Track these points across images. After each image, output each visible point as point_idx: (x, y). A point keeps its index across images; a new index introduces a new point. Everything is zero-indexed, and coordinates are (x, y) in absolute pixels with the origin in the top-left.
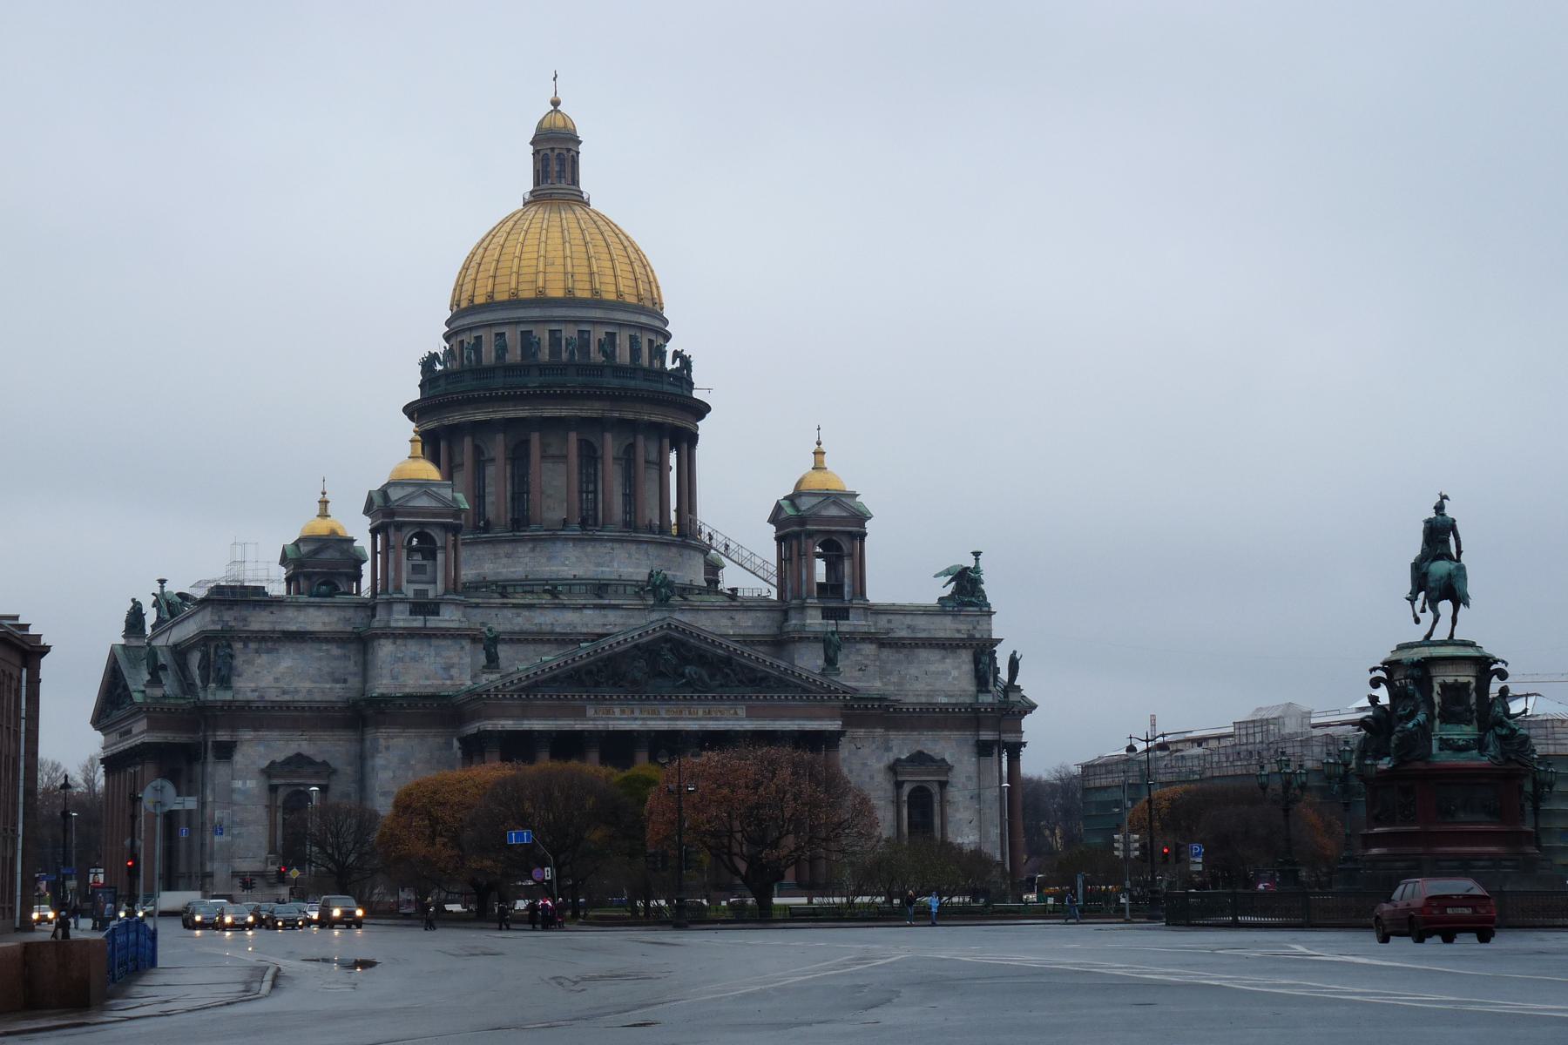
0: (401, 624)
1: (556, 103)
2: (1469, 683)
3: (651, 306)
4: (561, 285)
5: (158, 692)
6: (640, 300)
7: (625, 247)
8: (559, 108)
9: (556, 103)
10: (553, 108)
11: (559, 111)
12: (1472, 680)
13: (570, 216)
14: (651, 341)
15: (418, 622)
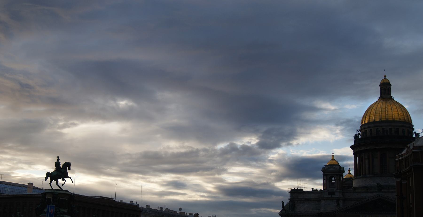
0: (326, 197)
1: (385, 77)
2: (50, 199)
3: (408, 122)
4: (385, 118)
5: (284, 212)
6: (405, 120)
7: (401, 108)
8: (386, 78)
9: (385, 77)
10: (384, 78)
11: (386, 78)
12: (51, 198)
13: (389, 102)
14: (408, 130)
15: (330, 196)
